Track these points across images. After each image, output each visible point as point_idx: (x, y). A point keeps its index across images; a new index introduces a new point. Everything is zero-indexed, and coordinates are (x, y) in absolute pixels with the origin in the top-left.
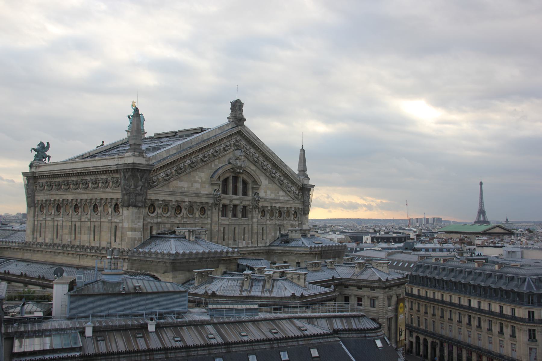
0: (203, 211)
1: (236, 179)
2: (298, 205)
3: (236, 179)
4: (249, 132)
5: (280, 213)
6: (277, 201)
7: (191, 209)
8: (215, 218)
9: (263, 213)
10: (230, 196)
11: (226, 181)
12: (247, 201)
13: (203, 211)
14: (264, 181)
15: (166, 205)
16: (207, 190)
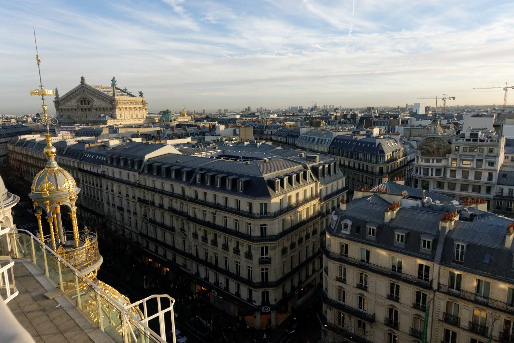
0: (75, 110)
1: (85, 100)
2: (111, 106)
3: (85, 100)
4: (88, 86)
5: (104, 109)
6: (101, 105)
7: (72, 110)
8: (79, 112)
9: (96, 109)
10: (84, 105)
11: (81, 101)
12: (89, 106)
13: (75, 110)
14: (95, 100)
15: (65, 109)
16: (76, 105)
